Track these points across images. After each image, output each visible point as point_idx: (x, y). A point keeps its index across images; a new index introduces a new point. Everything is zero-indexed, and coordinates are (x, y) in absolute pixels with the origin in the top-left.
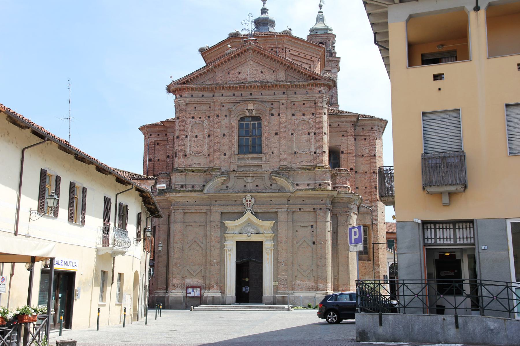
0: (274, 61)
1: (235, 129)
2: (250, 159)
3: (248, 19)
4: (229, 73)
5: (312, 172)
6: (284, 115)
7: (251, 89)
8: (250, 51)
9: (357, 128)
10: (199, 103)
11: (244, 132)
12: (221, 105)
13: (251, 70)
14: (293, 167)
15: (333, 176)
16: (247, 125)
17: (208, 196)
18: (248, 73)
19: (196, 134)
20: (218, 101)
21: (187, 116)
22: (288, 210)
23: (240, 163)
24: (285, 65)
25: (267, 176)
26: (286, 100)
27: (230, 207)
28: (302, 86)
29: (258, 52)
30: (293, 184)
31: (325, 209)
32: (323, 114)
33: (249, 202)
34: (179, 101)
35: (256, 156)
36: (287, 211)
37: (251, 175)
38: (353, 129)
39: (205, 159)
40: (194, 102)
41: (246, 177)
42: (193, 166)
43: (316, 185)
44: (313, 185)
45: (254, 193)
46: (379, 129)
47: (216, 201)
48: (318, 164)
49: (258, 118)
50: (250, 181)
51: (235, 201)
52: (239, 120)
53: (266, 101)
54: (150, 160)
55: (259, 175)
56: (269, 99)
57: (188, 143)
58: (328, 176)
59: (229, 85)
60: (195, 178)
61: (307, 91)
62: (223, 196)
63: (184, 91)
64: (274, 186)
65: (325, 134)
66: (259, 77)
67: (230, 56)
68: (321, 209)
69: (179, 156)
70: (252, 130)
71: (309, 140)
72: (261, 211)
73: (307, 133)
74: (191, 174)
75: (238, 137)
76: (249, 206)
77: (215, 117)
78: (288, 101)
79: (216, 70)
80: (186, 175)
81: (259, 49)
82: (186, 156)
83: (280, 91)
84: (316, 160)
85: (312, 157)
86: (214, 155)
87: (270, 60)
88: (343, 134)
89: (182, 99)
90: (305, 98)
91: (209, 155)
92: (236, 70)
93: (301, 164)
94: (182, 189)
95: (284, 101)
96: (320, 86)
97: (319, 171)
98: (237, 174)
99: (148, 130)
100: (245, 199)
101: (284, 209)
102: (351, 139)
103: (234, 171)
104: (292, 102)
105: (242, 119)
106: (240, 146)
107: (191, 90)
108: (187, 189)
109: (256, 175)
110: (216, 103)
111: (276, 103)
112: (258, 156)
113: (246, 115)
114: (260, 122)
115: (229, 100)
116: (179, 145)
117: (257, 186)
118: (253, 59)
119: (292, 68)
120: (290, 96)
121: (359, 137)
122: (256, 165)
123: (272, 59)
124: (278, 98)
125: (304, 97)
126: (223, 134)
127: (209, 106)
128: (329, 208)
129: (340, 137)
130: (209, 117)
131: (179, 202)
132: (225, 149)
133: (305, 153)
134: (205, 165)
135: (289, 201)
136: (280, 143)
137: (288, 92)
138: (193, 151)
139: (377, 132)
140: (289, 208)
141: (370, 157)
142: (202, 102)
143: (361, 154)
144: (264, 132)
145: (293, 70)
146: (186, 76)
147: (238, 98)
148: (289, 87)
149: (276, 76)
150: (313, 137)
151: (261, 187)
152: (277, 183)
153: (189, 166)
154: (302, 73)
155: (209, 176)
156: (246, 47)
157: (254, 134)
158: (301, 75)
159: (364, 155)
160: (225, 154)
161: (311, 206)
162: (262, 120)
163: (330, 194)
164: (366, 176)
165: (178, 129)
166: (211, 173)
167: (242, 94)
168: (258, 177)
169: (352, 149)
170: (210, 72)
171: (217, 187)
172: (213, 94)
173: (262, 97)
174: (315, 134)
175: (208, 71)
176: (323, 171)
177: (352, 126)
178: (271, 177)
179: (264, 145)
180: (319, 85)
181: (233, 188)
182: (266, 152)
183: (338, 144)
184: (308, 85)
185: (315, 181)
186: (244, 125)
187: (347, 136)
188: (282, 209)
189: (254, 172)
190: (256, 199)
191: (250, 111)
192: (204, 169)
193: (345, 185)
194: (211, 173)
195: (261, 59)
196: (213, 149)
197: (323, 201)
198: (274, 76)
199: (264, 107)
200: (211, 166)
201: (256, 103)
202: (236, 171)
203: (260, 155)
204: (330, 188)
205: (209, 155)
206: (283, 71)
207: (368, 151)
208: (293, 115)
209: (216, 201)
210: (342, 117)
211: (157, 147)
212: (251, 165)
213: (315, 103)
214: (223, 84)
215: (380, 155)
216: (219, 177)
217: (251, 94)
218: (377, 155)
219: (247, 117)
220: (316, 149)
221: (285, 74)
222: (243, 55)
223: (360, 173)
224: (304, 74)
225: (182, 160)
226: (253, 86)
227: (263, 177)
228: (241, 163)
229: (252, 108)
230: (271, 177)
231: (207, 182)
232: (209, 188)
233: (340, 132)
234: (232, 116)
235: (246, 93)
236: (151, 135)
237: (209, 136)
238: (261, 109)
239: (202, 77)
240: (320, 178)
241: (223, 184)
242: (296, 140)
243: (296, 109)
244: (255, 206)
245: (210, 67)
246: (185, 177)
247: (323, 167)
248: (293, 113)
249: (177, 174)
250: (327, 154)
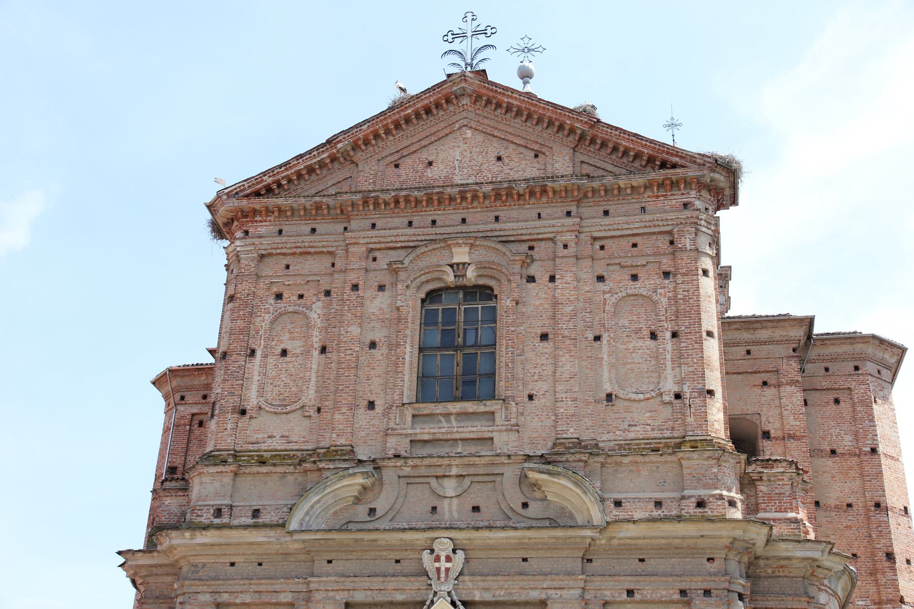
0: (537, 124)
1: (410, 325)
2: (453, 418)
3: (464, 26)
4: (397, 166)
5: (670, 458)
6: (569, 277)
7: (464, 204)
8: (466, 101)
9: (809, 367)
10: (301, 254)
11: (440, 336)
12: (367, 257)
13: (468, 155)
14: (601, 445)
15: (747, 483)
16: (450, 314)
17: (304, 541)
18: (457, 163)
19: (283, 346)
20: (358, 244)
21: (260, 293)
22: (587, 596)
23: (418, 431)
24: (572, 131)
25: (510, 473)
26: (577, 233)
27: (377, 582)
28: (629, 191)
29: (489, 102)
30: (603, 500)
31: (726, 593)
32: (700, 272)
33: (444, 565)
34: (238, 249)
35: (475, 407)
36: (582, 597)
37: (454, 471)
38: (795, 365)
39: (306, 422)
40: (283, 251)
41: (437, 477)
42: (263, 447)
43: (685, 502)
44: (675, 505)
45: (461, 529)
46: (879, 372)
47: (330, 562)
48: (691, 433)
49: (485, 292)
50: (450, 493)
51: (398, 561)
52: (423, 301)
53: (512, 238)
54: (172, 470)
55: (481, 471)
56: (520, 232)
57: (256, 373)
58: (731, 479)
59: (393, 194)
60: (265, 483)
61: (643, 205)
62: (356, 540)
63: (256, 219)
64: (535, 509)
65: (710, 334)
66: (490, 171)
67: (402, 114)
68: (707, 593)
69: (223, 412)
70: (465, 330)
71: (657, 357)
72: (488, 597)
73: (646, 333)
74: (256, 469)
75: (416, 351)
76: (443, 580)
77: (348, 290)
78: (582, 236)
79: (359, 156)
80: (236, 474)
81: (492, 90)
82: (243, 412)
83: (555, 210)
84: (684, 420)
85: (666, 412)
86: (336, 408)
87: (526, 121)
88: (765, 379)
89: (249, 241)
90: (637, 225)
91: (319, 410)
92: (418, 155)
93: (631, 435)
94: (217, 521)
95: (569, 237)
96: (685, 188)
97: (695, 455)
98: (409, 469)
99: (175, 383)
100: (432, 551)
101: (572, 592)
102: (793, 396)
103: (397, 456)
104: (595, 239)
105: (432, 296)
106: (424, 380)
107: (276, 214)
108: (236, 522)
109: (472, 471)
110: (352, 249)
111: (543, 243)
112: (482, 409)
113: (446, 282)
114: (491, 304)
115: (393, 239)
116: (224, 380)
117: (476, 509)
118: (473, 124)
119: (593, 141)
120: (585, 223)
121: (817, 394)
122: (472, 436)
123: (529, 116)
124: (552, 229)
125: (637, 223)
126: (368, 342)
127: (331, 260)
128: (741, 591)
129: (756, 389)
130: (328, 293)
131: (204, 565)
132: (374, 389)
133: (641, 396)
134: (304, 442)
135: (590, 561)
136: (555, 365)
137: (581, 210)
138: (269, 396)
139: (874, 379)
140: (590, 586)
141: (859, 456)
142: (310, 250)
143: (828, 449)
144: (502, 331)
145: (597, 147)
146: (264, 174)
147: (424, 232)
148: (585, 196)
149: (543, 167)
150: (670, 344)
151: (489, 512)
152: (544, 499)
153: (250, 447)
154: (626, 152)
155: (313, 476)
156: (452, 86)
157: (471, 341)
158: (625, 160)
159: (838, 451)
160: (371, 405)
161: (670, 579)
162: (496, 296)
163: (738, 533)
164: (850, 518)
165: (228, 330)
166: (321, 465)
167: (434, 222)
168: (480, 478)
169: (798, 423)
170: (341, 163)
171: (335, 513)
172: (346, 225)
173: (497, 226)
174: (674, 335)
175: (333, 159)
176: (708, 454)
177: (792, 353)
178: (523, 477)
179: (502, 373)
180: (682, 186)
181: (390, 516)
182: (509, 393)
183: (751, 409)
184: (648, 186)
185: (683, 489)
186: (440, 315)
187: (778, 386)
188: (564, 592)
189: (466, 461)
190: (472, 554)
191: (459, 268)
192: (299, 453)
193: (791, 515)
194: (321, 465)
195: (497, 122)
196: (333, 389)
197: (716, 563)
198: (538, 166)
199: (504, 254)
200: (322, 444)
201: (478, 243)
202: (407, 458)
203: (488, 403)
204: (737, 514)
205: (319, 410)
206: (567, 152)
207: (849, 438)
208: (601, 278)
209: (330, 562)
210: (758, 325)
211: (197, 431)
212: (458, 436)
213: (672, 243)
214: (374, 191)
215: (891, 452)
216: (344, 476)
217: (464, 221)
218: (881, 449)
219: (447, 289)
220: (681, 382)
221: (573, 161)
222: (441, 113)
223: (827, 508)
224: (632, 154)
225: (229, 426)
226: (469, 195)
227: (498, 479)
228: (425, 431)
229: (465, 259)
230: (523, 477)
231: (303, 492)
232: (307, 513)
233: (755, 372)
234: (400, 286)
235: (449, 217)
236: (183, 398)
237: (323, 350)
238: (493, 263)
239: (314, 177)
240: (699, 479)
241: (358, 500)
242: (609, 355)
243: (609, 262)
244: (466, 578)
245: (339, 146)
246: (234, 480)
247: (710, 442)
248: (600, 272)
249: (205, 470)
250: (721, 401)
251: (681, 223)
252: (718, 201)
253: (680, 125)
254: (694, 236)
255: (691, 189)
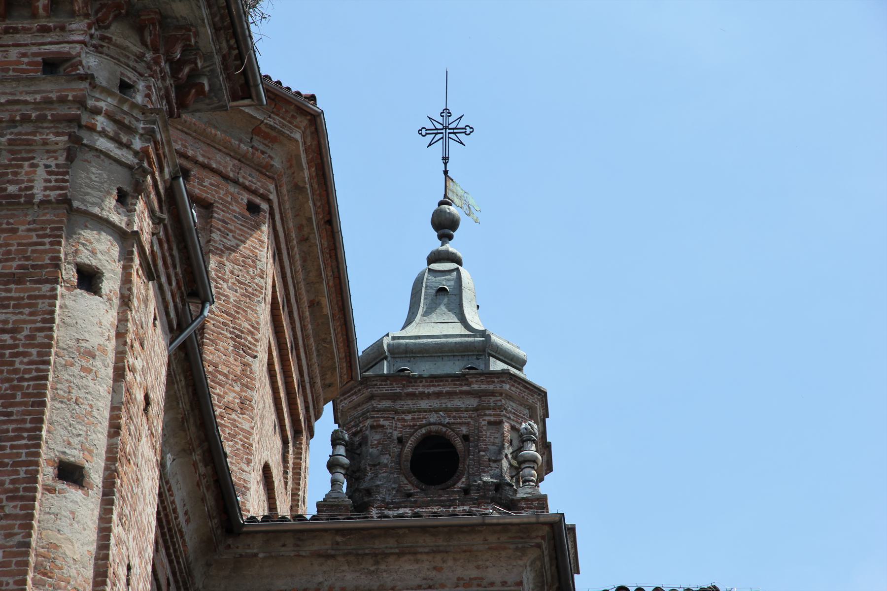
32: (69, 273)
210: (389, 544)
251: (26, 119)
252: (176, 66)
253: (468, 130)
254: (62, 160)
255: (73, 14)
